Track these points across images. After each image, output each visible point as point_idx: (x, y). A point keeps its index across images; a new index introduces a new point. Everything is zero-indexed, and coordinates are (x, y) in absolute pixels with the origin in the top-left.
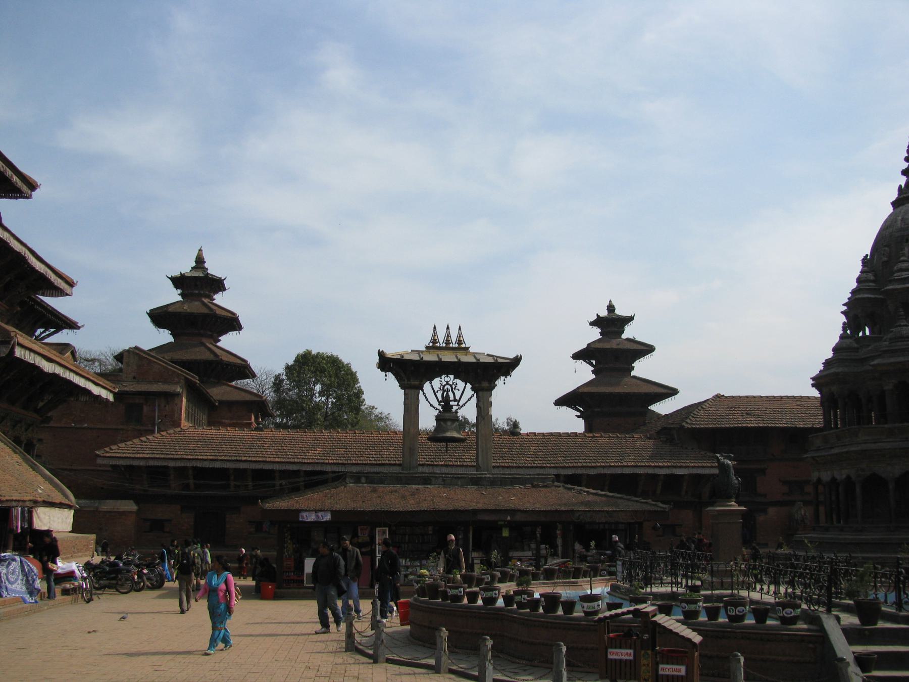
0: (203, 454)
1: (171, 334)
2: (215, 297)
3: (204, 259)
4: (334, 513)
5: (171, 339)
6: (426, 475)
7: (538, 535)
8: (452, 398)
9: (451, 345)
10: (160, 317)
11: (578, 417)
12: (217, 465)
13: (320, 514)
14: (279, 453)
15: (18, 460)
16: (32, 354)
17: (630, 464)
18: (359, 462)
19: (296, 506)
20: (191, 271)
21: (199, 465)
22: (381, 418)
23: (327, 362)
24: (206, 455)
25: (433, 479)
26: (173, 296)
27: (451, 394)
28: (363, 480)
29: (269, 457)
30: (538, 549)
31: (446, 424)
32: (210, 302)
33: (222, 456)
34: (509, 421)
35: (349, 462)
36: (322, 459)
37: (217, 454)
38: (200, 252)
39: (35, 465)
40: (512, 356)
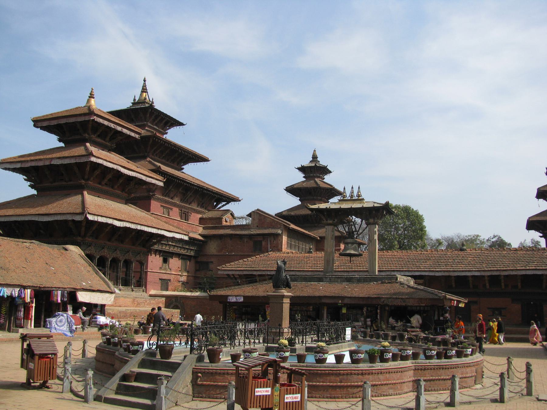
4: (245, 297)
5: (300, 203)
6: (321, 276)
7: (365, 313)
9: (354, 198)
10: (292, 190)
11: (541, 237)
13: (238, 298)
15: (89, 270)
17: (531, 268)
22: (483, 242)
25: (324, 279)
26: (299, 178)
27: (353, 227)
30: (365, 322)
31: (348, 245)
34: (533, 241)
39: (98, 272)
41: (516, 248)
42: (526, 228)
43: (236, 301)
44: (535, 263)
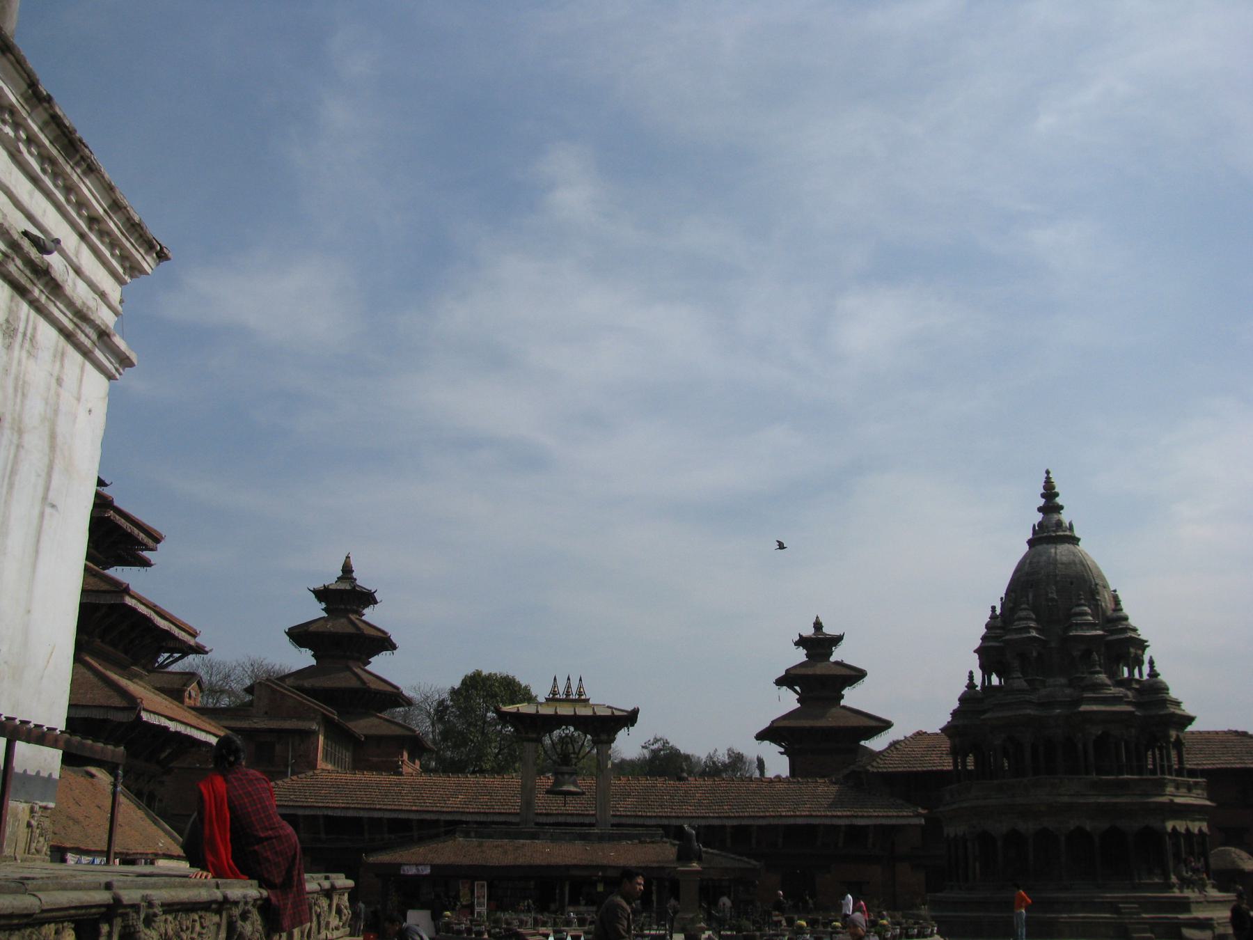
0: (334, 801)
1: (313, 656)
2: (366, 611)
4: (433, 867)
5: (313, 662)
8: (571, 751)
10: (300, 636)
11: (782, 753)
12: (350, 814)
13: (420, 868)
14: (417, 801)
16: (156, 716)
18: (502, 811)
19: (399, 860)
20: (336, 582)
21: (330, 813)
23: (501, 683)
24: (338, 803)
26: (315, 611)
28: (473, 834)
29: (406, 805)
32: (357, 619)
33: (355, 803)
34: (730, 752)
35: (492, 811)
36: (463, 808)
37: (350, 802)
38: (348, 559)
40: (630, 708)
41: (771, 778)
42: (757, 735)
43: (417, 873)
44: (808, 806)
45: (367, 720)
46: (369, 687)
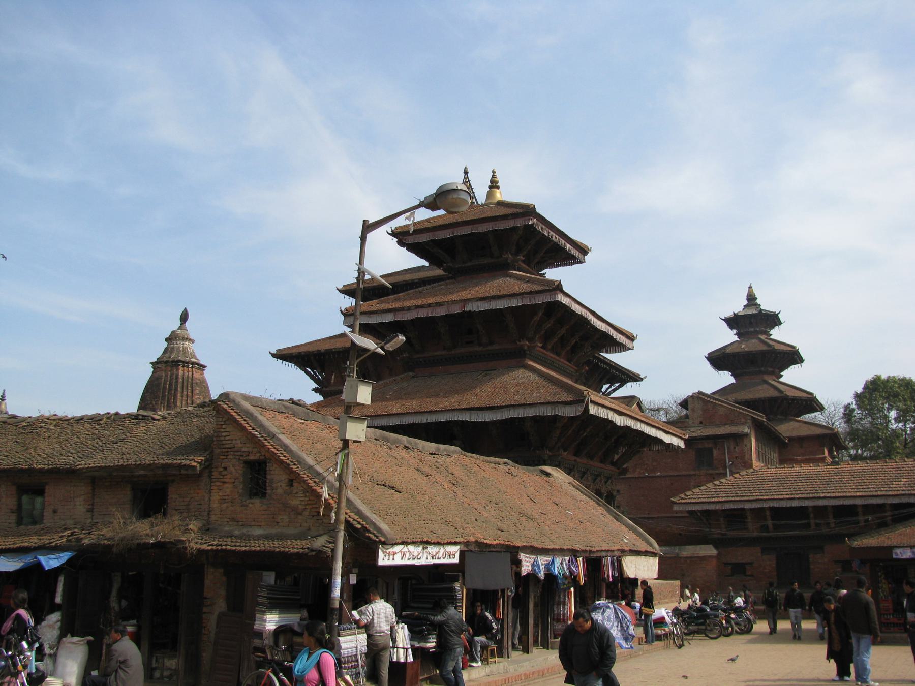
1: (731, 375)
2: (772, 332)
3: (755, 296)
5: (732, 380)
10: (719, 360)
12: (795, 504)
14: (860, 487)
15: (603, 512)
16: (605, 410)
19: (887, 543)
20: (743, 309)
21: (776, 505)
23: (900, 385)
24: (782, 495)
26: (728, 337)
29: (849, 492)
37: (794, 493)
38: (751, 289)
39: (619, 515)
45: (787, 424)
46: (786, 395)
